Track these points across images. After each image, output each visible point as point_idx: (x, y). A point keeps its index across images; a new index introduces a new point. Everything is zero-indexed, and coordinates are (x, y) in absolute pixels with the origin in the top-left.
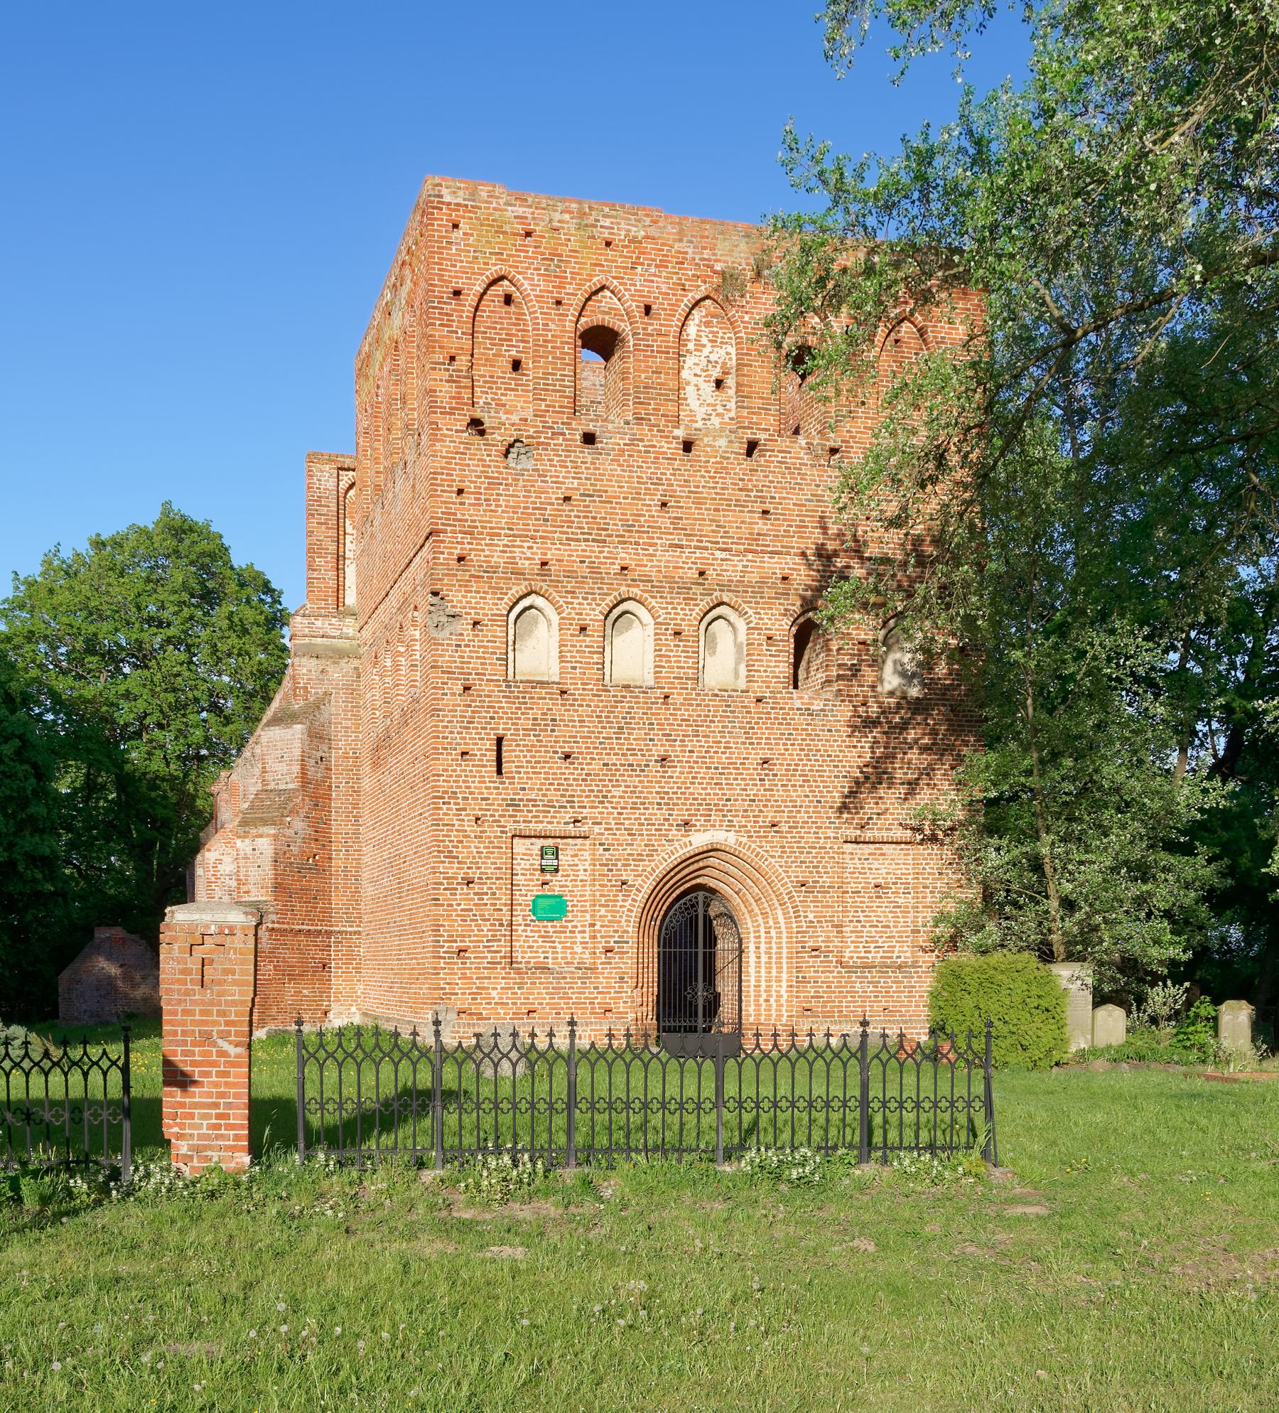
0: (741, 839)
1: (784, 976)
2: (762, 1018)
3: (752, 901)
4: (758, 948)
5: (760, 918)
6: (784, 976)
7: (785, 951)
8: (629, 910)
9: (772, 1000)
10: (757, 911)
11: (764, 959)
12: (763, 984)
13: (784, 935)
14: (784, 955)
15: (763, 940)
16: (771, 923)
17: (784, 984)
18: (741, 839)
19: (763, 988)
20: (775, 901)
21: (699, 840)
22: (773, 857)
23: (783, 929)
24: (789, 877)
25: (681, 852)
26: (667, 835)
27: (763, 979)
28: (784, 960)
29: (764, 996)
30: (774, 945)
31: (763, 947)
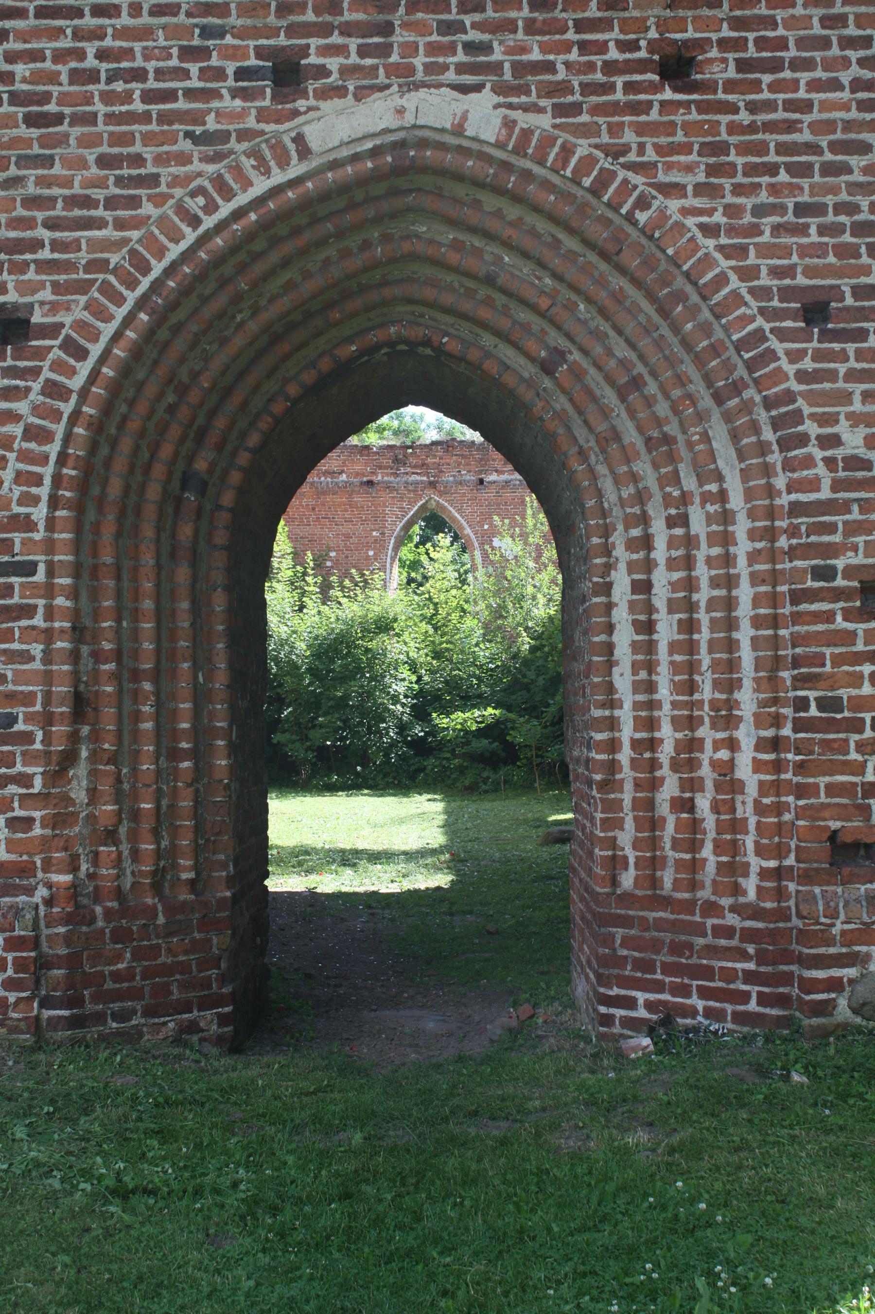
0: (524, 120)
1: (747, 699)
2: (668, 877)
3: (610, 397)
4: (643, 587)
5: (643, 467)
6: (747, 699)
7: (745, 593)
8: (30, 433)
9: (703, 803)
10: (631, 436)
11: (666, 630)
12: (667, 732)
13: (741, 527)
14: (744, 610)
15: (660, 553)
16: (689, 483)
17: (746, 735)
18: (524, 120)
19: (666, 752)
20: (698, 387)
21: (340, 126)
22: (677, 190)
23: (736, 501)
24: (747, 274)
25: (260, 186)
26: (198, 118)
27: (665, 712)
28: (745, 634)
29: (670, 788)
30: (702, 572)
31: (662, 579)
